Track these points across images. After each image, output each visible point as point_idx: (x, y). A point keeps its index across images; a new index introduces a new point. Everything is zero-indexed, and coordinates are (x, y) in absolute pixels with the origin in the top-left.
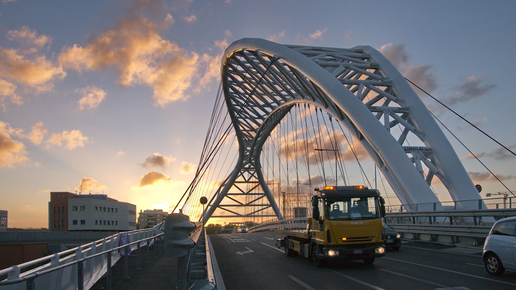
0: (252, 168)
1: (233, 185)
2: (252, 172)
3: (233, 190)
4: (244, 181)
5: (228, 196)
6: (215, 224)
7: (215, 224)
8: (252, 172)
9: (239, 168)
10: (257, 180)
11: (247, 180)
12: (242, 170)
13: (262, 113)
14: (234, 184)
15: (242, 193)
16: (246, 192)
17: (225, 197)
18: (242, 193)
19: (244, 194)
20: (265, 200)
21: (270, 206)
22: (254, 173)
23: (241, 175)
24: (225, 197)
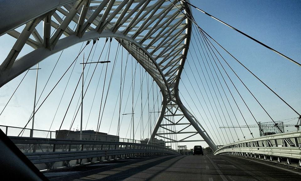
0: (174, 105)
2: (177, 107)
3: (164, 121)
9: (165, 104)
12: (177, 106)
13: (157, 53)
19: (174, 124)
20: (192, 129)
21: (197, 133)
22: (178, 108)
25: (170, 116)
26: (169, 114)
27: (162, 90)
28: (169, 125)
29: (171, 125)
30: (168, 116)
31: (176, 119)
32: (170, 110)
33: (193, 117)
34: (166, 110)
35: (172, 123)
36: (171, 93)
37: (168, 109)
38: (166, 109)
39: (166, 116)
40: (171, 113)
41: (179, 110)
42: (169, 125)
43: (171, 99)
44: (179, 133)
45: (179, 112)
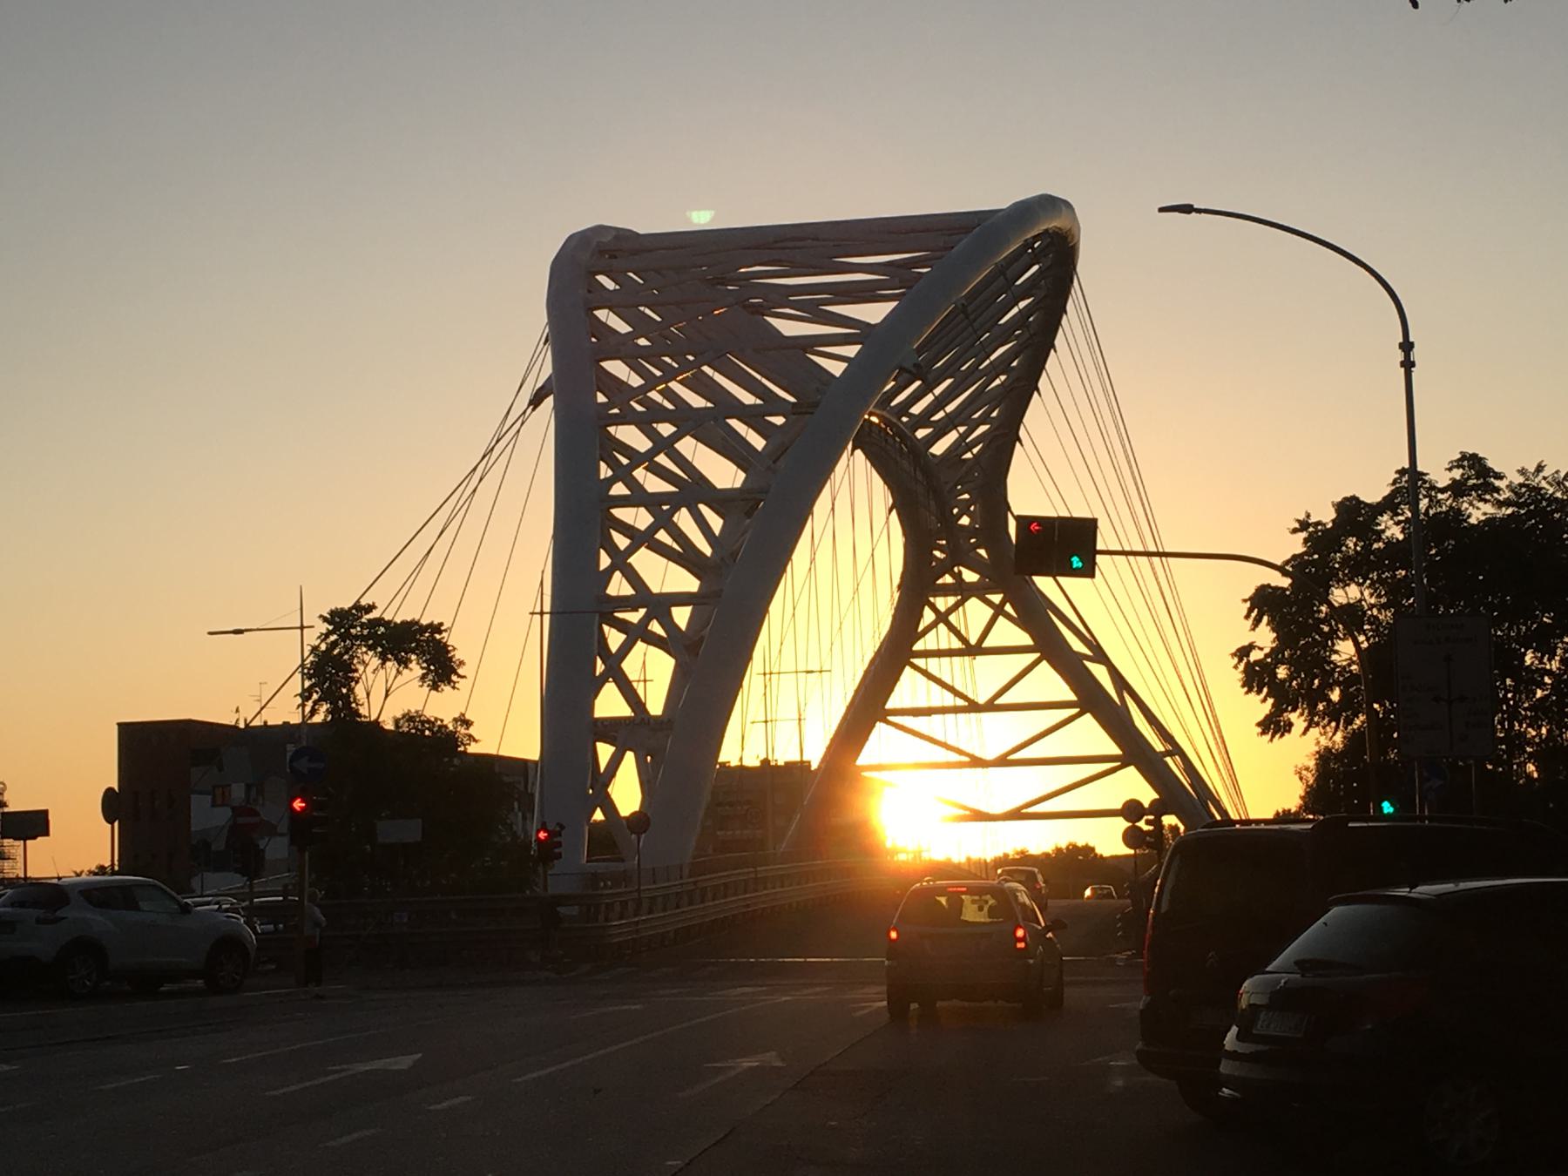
1: (908, 669)
3: (909, 689)
4: (956, 644)
5: (890, 718)
8: (996, 598)
10: (1025, 639)
11: (973, 641)
14: (916, 661)
15: (961, 702)
16: (982, 699)
17: (880, 726)
18: (966, 704)
19: (973, 707)
21: (1124, 761)
22: (1003, 603)
23: (942, 627)
25: (950, 653)
26: (944, 646)
27: (904, 505)
29: (956, 710)
30: (939, 653)
31: (983, 677)
32: (952, 618)
33: (1100, 656)
34: (928, 616)
35: (961, 702)
36: (965, 521)
37: (933, 608)
38: (927, 609)
41: (1008, 616)
44: (1003, 761)
45: (1008, 633)
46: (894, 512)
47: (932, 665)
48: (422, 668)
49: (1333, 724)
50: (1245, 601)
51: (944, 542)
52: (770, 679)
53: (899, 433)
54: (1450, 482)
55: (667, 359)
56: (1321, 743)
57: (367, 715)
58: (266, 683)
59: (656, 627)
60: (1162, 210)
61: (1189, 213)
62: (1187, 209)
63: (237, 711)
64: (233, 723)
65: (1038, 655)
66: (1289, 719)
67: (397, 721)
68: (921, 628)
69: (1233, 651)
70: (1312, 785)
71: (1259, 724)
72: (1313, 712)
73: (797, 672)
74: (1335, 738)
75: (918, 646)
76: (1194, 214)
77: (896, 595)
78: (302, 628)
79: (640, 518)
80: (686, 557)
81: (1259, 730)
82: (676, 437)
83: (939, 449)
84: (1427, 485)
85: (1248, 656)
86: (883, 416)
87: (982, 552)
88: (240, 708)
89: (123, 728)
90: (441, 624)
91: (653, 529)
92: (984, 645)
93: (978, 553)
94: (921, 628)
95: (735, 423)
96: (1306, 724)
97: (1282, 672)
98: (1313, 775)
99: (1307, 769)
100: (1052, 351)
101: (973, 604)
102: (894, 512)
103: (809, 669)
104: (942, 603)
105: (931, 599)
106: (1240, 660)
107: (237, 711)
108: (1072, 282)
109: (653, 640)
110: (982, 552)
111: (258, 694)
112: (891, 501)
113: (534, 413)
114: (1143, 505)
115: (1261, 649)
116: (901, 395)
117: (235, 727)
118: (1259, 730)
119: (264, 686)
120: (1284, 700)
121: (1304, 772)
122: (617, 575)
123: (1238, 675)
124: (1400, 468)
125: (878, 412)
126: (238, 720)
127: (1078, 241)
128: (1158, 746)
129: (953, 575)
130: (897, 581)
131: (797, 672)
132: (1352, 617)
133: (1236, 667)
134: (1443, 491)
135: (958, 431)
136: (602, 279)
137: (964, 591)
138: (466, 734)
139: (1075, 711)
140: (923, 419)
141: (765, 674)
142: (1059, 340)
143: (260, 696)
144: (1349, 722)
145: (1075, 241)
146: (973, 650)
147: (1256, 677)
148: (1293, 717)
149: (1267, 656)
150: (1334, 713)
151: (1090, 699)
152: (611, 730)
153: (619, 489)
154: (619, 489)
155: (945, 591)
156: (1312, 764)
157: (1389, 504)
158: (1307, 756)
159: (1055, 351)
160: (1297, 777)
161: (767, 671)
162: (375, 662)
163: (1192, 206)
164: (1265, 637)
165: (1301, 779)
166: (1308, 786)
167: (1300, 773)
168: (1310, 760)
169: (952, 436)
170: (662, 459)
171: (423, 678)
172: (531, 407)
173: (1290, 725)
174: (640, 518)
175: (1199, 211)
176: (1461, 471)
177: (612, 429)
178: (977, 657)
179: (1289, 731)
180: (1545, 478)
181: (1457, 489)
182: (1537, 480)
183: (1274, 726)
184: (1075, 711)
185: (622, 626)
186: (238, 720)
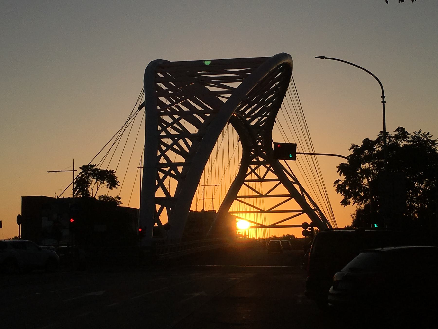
3: (243, 191)
4: (257, 178)
6: (286, 235)
7: (286, 235)
8: (268, 166)
10: (276, 177)
11: (261, 178)
16: (264, 194)
17: (235, 201)
19: (261, 196)
22: (270, 167)
23: (253, 173)
24: (235, 201)
25: (255, 181)
26: (253, 179)
27: (243, 139)
28: (253, 197)
29: (256, 197)
30: (252, 181)
31: (265, 187)
32: (256, 171)
33: (297, 182)
34: (249, 170)
35: (258, 194)
36: (260, 144)
37: (251, 168)
39: (248, 181)
40: (256, 177)
41: (271, 171)
42: (253, 197)
43: (258, 153)
44: (269, 211)
45: (271, 175)
46: (240, 141)
47: (250, 184)
48: (107, 183)
49: (361, 202)
50: (337, 167)
51: (254, 150)
52: (205, 187)
53: (242, 118)
54: (395, 135)
55: (177, 97)
56: (358, 207)
57: (92, 196)
58: (63, 186)
59: (173, 172)
60: (316, 58)
61: (323, 59)
62: (323, 58)
63: (55, 194)
64: (54, 197)
65: (280, 181)
66: (349, 201)
67: (100, 197)
68: (247, 173)
69: (334, 182)
70: (355, 219)
71: (341, 203)
72: (355, 198)
73: (212, 185)
74: (361, 206)
75: (246, 179)
76: (325, 59)
77: (240, 164)
78: (74, 171)
79: (169, 142)
80: (182, 152)
81: (341, 204)
82: (179, 119)
83: (253, 123)
84: (388, 136)
85: (338, 183)
86: (238, 114)
87: (264, 152)
88: (56, 193)
89: (23, 198)
90: (113, 171)
91: (172, 145)
92: (264, 179)
93: (264, 153)
94: (247, 173)
95: (195, 115)
96: (354, 202)
97: (347, 188)
98: (355, 216)
99: (354, 215)
100: (285, 97)
101: (262, 167)
102: (240, 141)
103: (216, 184)
104: (253, 167)
105: (250, 165)
106: (335, 184)
107: (55, 194)
108: (291, 77)
109: (172, 176)
110: (264, 152)
111: (61, 189)
112: (239, 138)
113: (140, 112)
114: (309, 140)
115: (342, 181)
116: (243, 108)
117: (55, 198)
118: (341, 204)
119: (63, 187)
120: (347, 195)
121: (353, 216)
122: (162, 157)
123: (335, 188)
124: (381, 131)
125: (235, 113)
126: (55, 197)
127: (293, 66)
128: (313, 208)
129: (256, 159)
130: (240, 160)
131: (212, 185)
132: (367, 172)
133: (334, 186)
134: (393, 137)
135: (258, 119)
136: (159, 74)
137: (259, 164)
138: (119, 201)
139: (290, 197)
140: (249, 115)
141: (203, 186)
142: (287, 94)
143: (62, 190)
144: (366, 202)
145: (292, 65)
146: (261, 180)
147: (340, 189)
148: (351, 200)
149: (343, 183)
150: (361, 199)
151: (294, 194)
152: (160, 201)
153: (163, 133)
154: (163, 133)
155: (254, 163)
156: (355, 213)
157: (377, 141)
158: (354, 211)
159: (286, 97)
160: (351, 216)
161: (204, 185)
162: (94, 181)
163: (324, 57)
164: (343, 178)
165: (352, 217)
166: (354, 219)
167: (352, 216)
168: (355, 212)
169: (257, 120)
170: (175, 125)
171: (107, 185)
172: (139, 110)
173: (350, 202)
174: (169, 142)
175: (326, 58)
176: (398, 132)
177: (161, 116)
178: (263, 182)
179: (349, 204)
180: (421, 134)
181: (397, 137)
182: (419, 135)
183: (345, 203)
184: (290, 197)
185: (163, 172)
186: (55, 197)
